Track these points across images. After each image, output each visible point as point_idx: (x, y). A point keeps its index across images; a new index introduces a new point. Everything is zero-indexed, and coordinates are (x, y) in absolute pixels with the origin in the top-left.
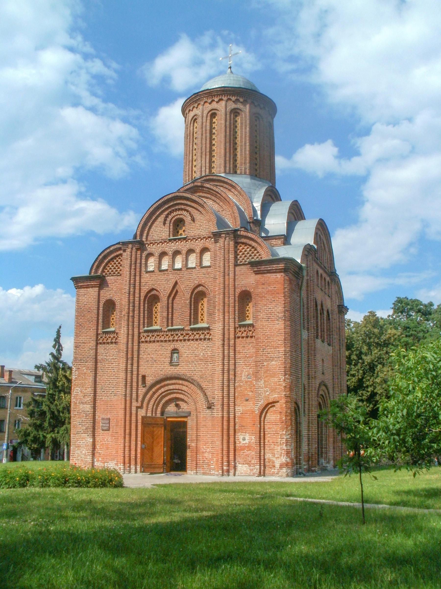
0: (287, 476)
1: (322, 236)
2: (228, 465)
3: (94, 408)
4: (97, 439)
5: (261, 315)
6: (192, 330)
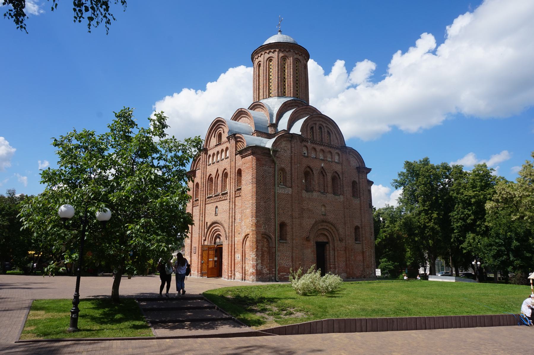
0: (257, 281)
1: (324, 125)
2: (231, 273)
3: (191, 241)
4: (193, 257)
5: (243, 182)
6: (222, 194)
